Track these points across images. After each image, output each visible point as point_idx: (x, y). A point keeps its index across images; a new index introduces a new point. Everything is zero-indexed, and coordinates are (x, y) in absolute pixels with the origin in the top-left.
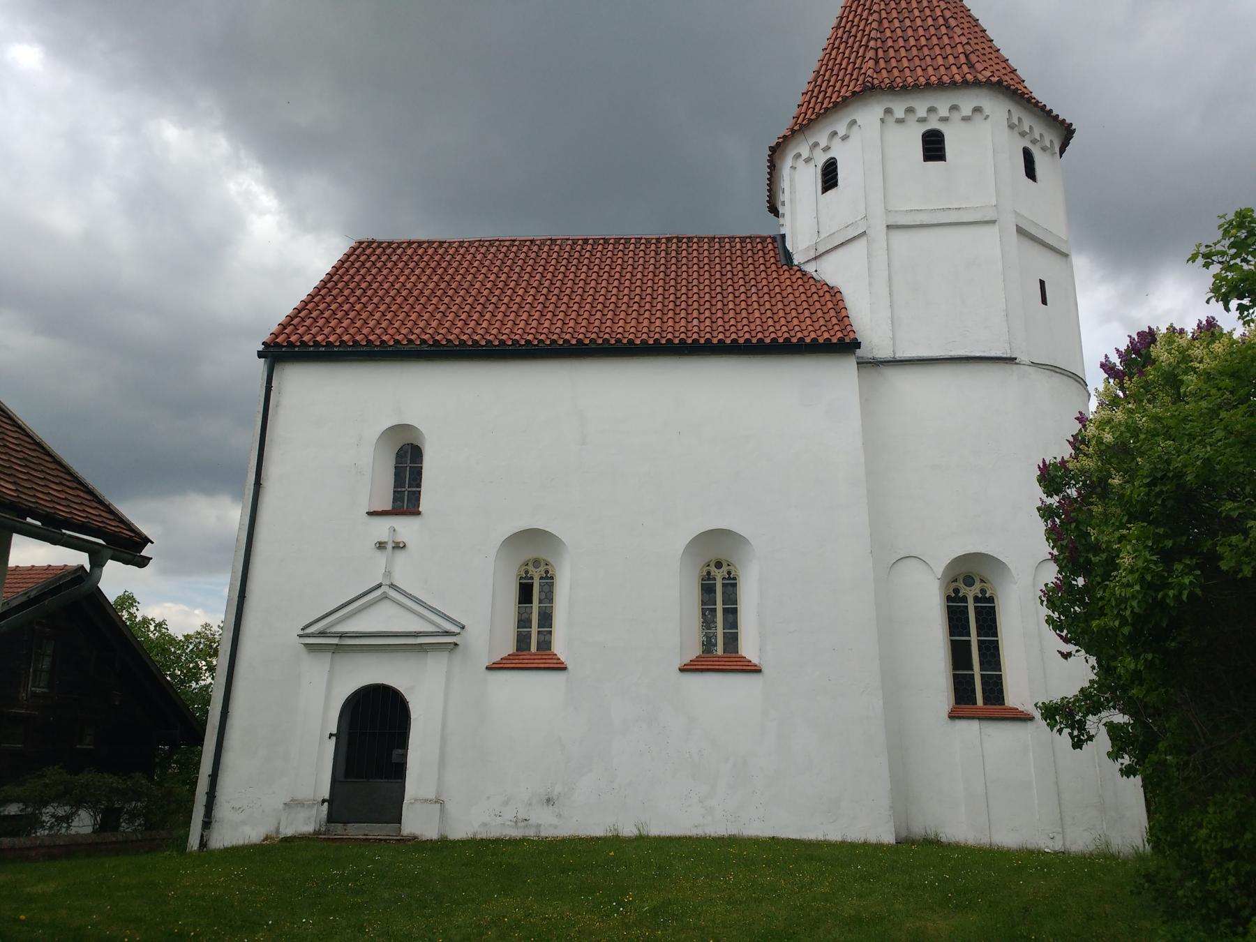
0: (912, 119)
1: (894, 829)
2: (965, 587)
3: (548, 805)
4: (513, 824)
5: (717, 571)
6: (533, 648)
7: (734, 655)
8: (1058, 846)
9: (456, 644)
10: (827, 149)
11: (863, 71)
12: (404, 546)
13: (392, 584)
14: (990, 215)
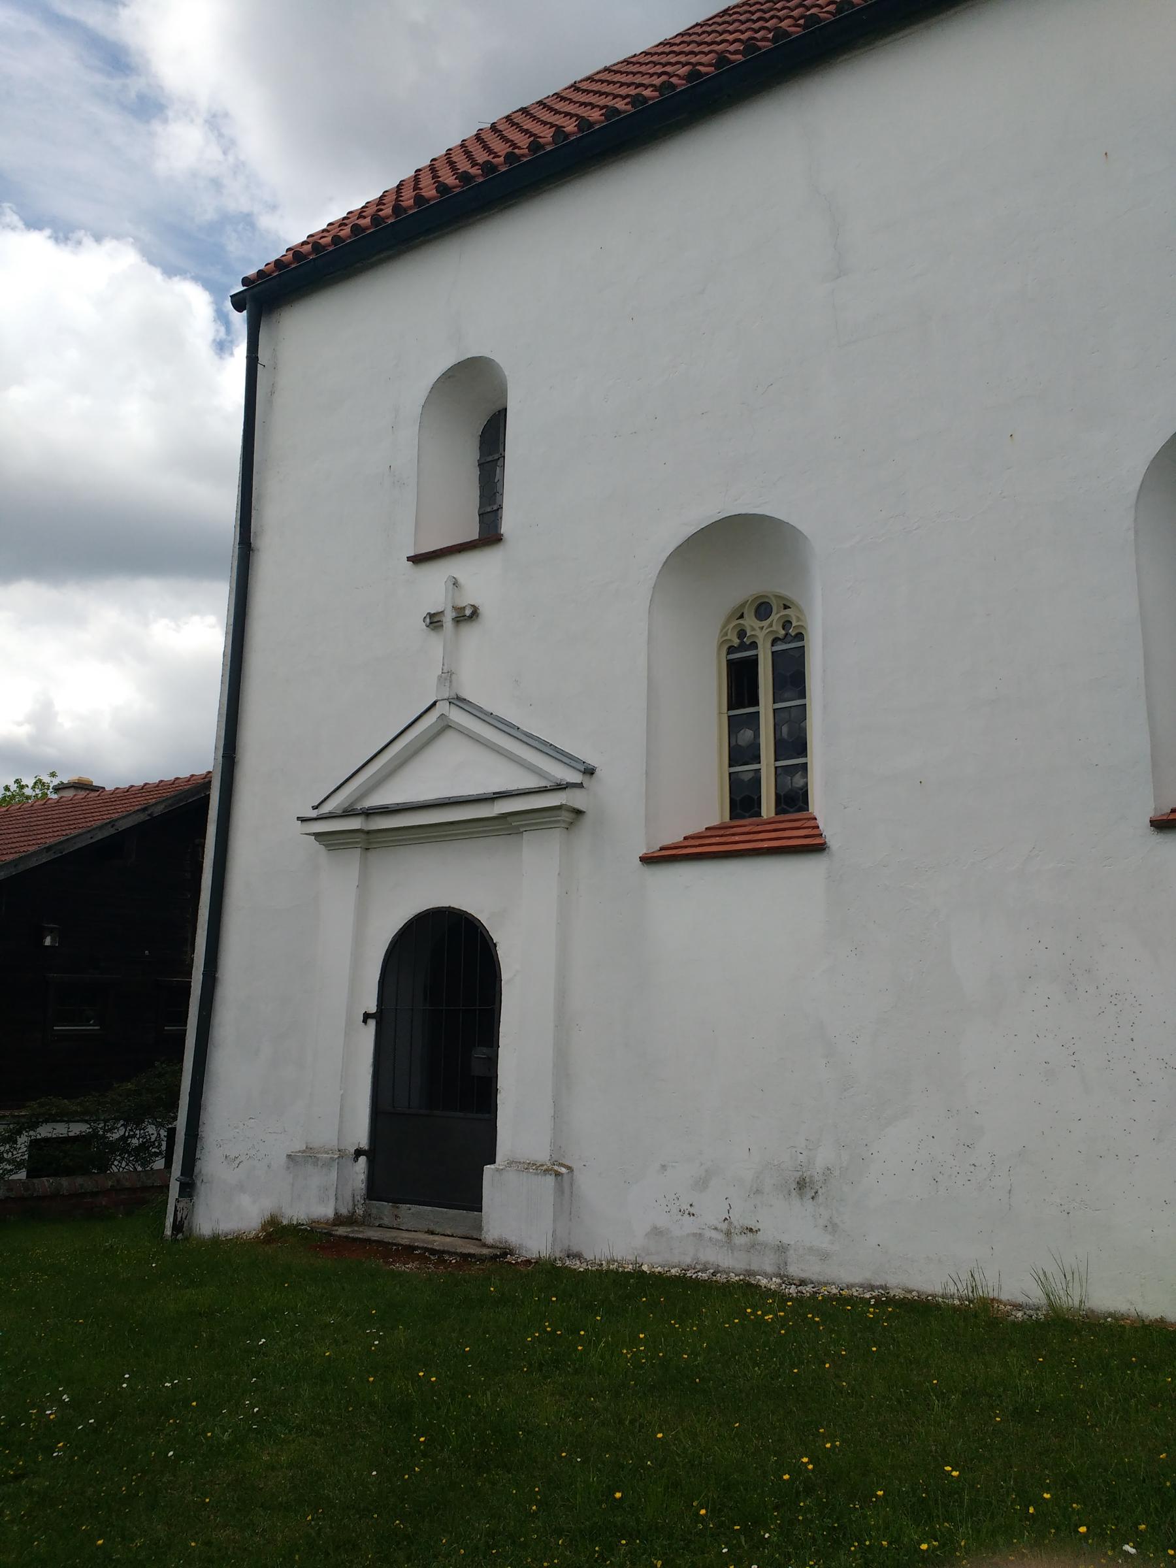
3: (801, 1196)
4: (720, 1236)
6: (768, 807)
9: (579, 813)
13: (458, 698)
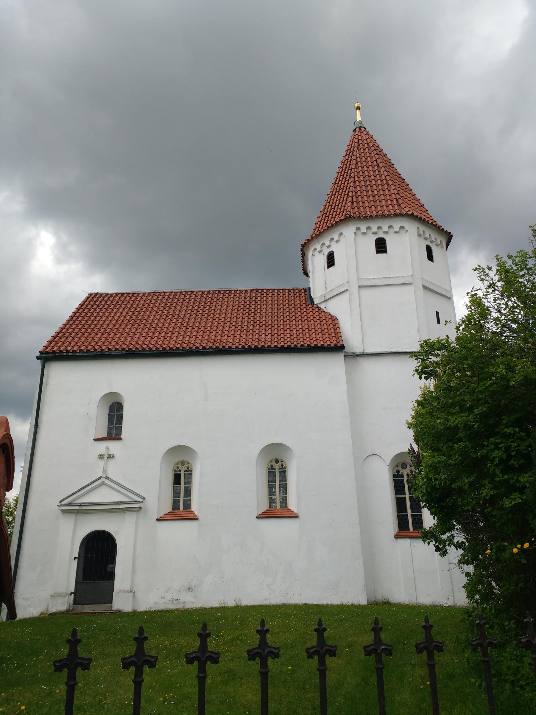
0: (370, 232)
1: (366, 597)
2: (402, 469)
3: (189, 591)
5: (276, 464)
7: (285, 508)
8: (450, 603)
9: (140, 508)
10: (329, 247)
11: (346, 208)
12: (113, 456)
13: (107, 477)
14: (409, 280)
